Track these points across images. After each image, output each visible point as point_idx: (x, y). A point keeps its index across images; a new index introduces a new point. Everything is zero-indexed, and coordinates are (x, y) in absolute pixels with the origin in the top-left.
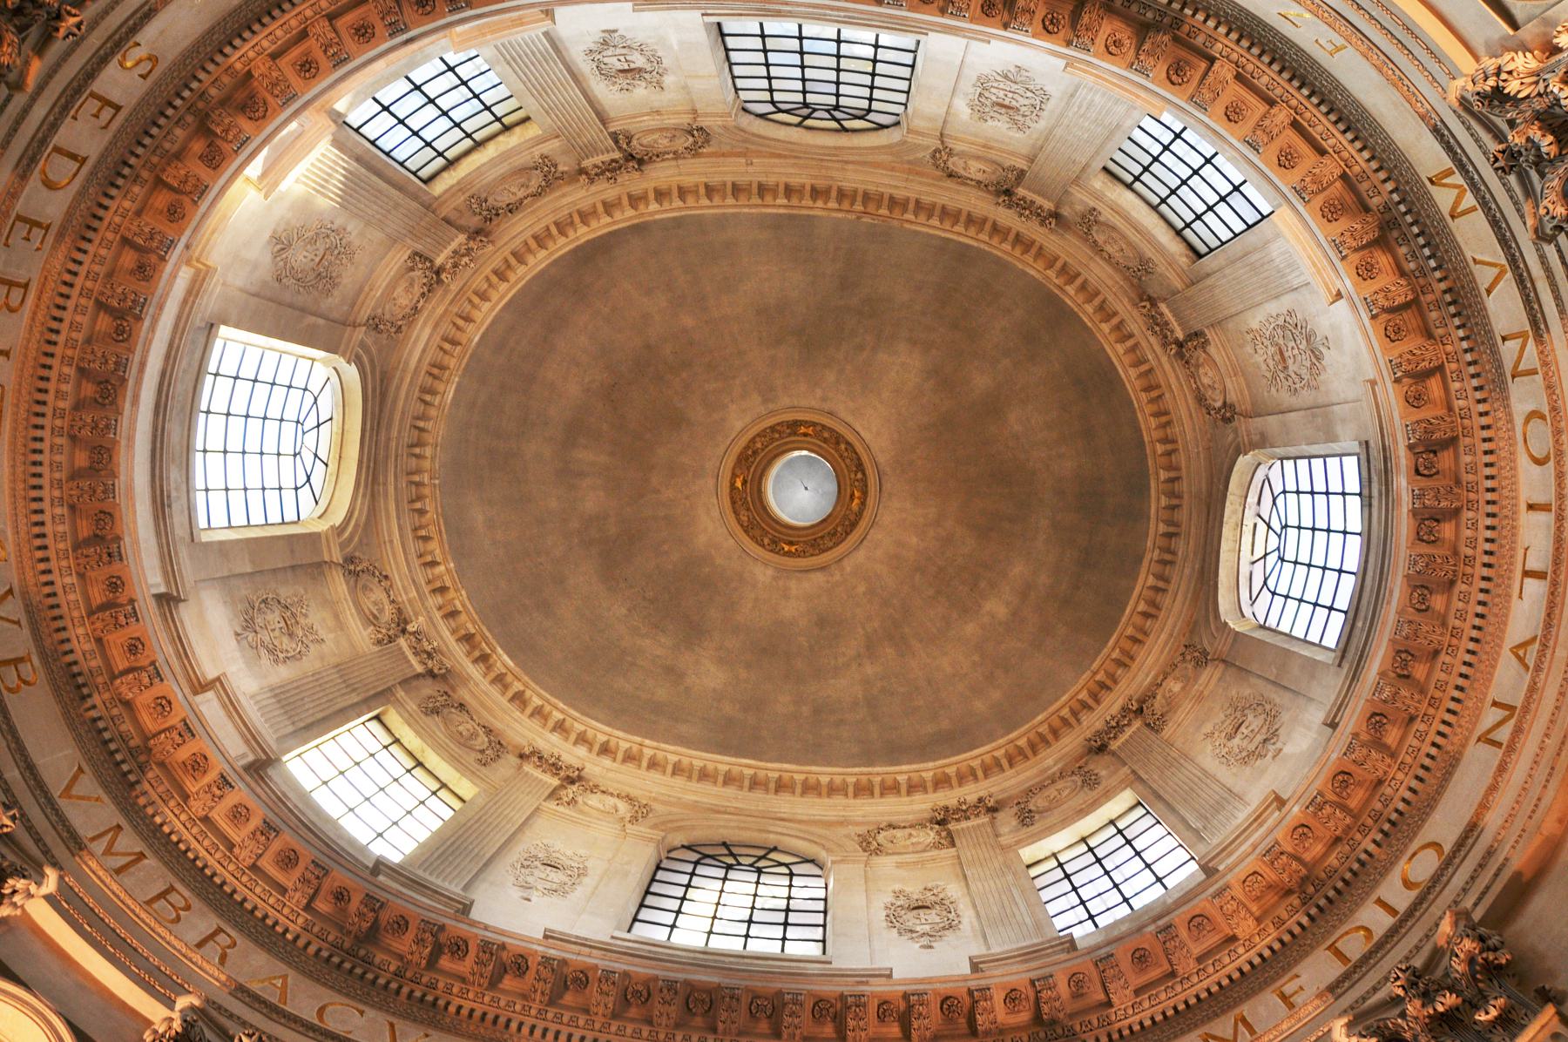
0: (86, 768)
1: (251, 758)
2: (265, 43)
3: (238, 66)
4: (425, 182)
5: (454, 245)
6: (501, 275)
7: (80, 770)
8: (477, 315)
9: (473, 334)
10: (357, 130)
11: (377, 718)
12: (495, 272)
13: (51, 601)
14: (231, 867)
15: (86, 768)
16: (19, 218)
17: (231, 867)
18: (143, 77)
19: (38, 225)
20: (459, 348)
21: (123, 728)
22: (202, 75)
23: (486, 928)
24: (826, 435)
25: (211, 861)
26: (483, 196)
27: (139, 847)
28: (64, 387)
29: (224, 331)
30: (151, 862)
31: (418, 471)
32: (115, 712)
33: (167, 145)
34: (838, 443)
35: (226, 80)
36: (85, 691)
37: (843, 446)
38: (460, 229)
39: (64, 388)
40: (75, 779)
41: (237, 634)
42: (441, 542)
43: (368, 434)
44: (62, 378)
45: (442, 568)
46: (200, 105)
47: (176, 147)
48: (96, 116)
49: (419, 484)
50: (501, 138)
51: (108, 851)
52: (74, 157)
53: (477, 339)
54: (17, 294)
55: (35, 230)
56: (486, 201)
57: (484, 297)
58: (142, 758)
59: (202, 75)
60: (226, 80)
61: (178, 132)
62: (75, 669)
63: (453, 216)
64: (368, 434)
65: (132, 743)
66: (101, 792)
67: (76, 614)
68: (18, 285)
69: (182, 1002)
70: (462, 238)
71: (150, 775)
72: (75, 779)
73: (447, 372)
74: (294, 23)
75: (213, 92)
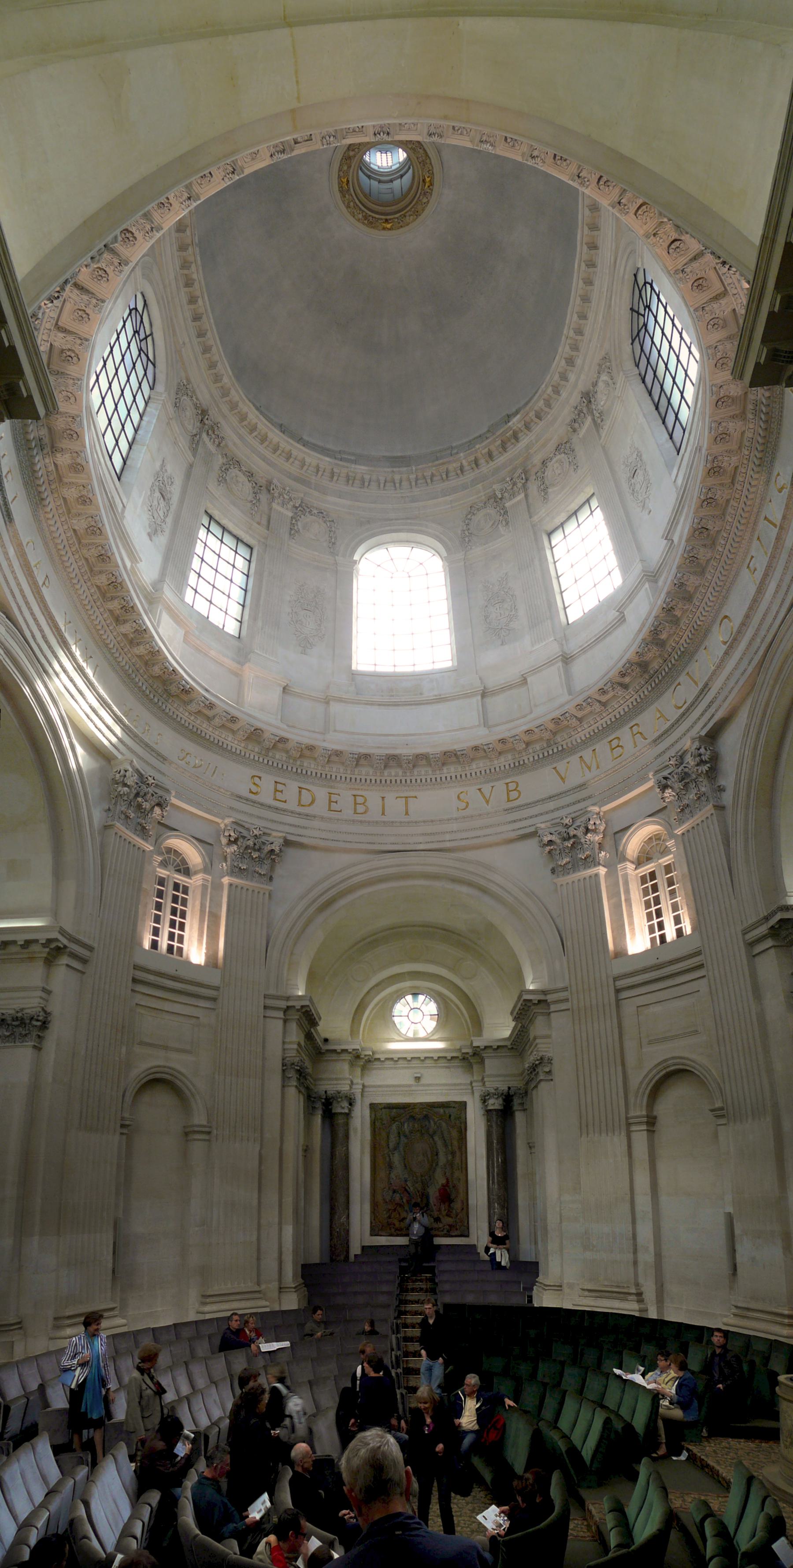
0: (554, 766)
1: (560, 664)
2: (230, 739)
3: (243, 745)
4: (251, 548)
5: (279, 508)
6: (288, 456)
7: (555, 768)
8: (314, 463)
9: (326, 461)
10: (241, 622)
11: (549, 535)
12: (288, 459)
13: (483, 772)
14: (604, 715)
15: (554, 766)
16: (330, 810)
17: (604, 715)
18: (260, 778)
19: (330, 797)
20: (335, 470)
21: (538, 748)
22: (252, 757)
23: (646, 619)
24: (345, 168)
25: (600, 722)
26: (249, 505)
27: (590, 750)
28: (393, 774)
29: (354, 667)
30: (597, 747)
31: (409, 480)
32: (531, 751)
33: (284, 759)
34: (350, 158)
35: (250, 747)
36: (522, 763)
37: (351, 153)
38: (271, 509)
39: (394, 773)
40: (557, 772)
41: (502, 644)
42: (449, 462)
43: (392, 528)
44: (390, 775)
45: (465, 463)
46: (263, 752)
47: (284, 755)
48: (282, 792)
49: (417, 479)
50: (217, 518)
51: (589, 768)
52: (300, 792)
53: (328, 459)
54: (360, 800)
55: (333, 799)
56: (251, 501)
57: (303, 464)
58: (552, 742)
59: (252, 757)
60: (250, 747)
61: (277, 757)
62: (512, 766)
63: (264, 522)
64: (392, 528)
65: (545, 745)
66: (566, 761)
67: (489, 764)
68: (355, 800)
69: (651, 777)
70: (275, 506)
71: (559, 740)
72: (557, 772)
73: (350, 474)
74: (217, 733)
75: (256, 750)
